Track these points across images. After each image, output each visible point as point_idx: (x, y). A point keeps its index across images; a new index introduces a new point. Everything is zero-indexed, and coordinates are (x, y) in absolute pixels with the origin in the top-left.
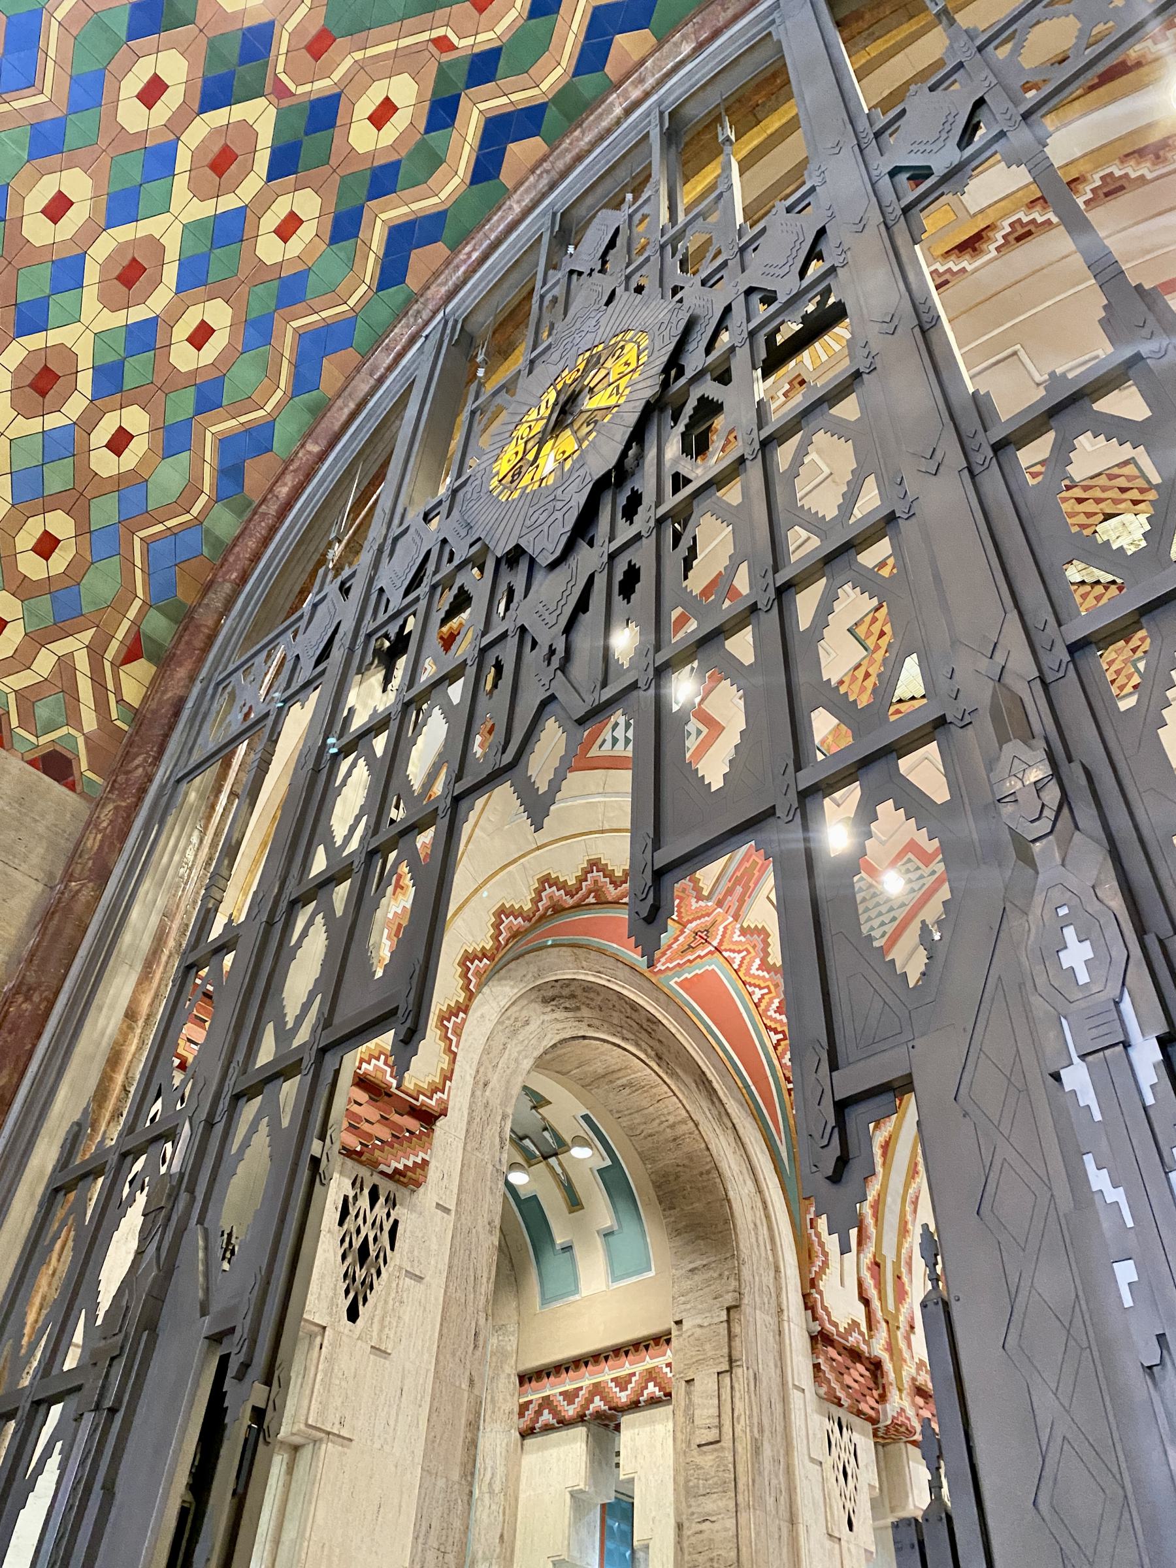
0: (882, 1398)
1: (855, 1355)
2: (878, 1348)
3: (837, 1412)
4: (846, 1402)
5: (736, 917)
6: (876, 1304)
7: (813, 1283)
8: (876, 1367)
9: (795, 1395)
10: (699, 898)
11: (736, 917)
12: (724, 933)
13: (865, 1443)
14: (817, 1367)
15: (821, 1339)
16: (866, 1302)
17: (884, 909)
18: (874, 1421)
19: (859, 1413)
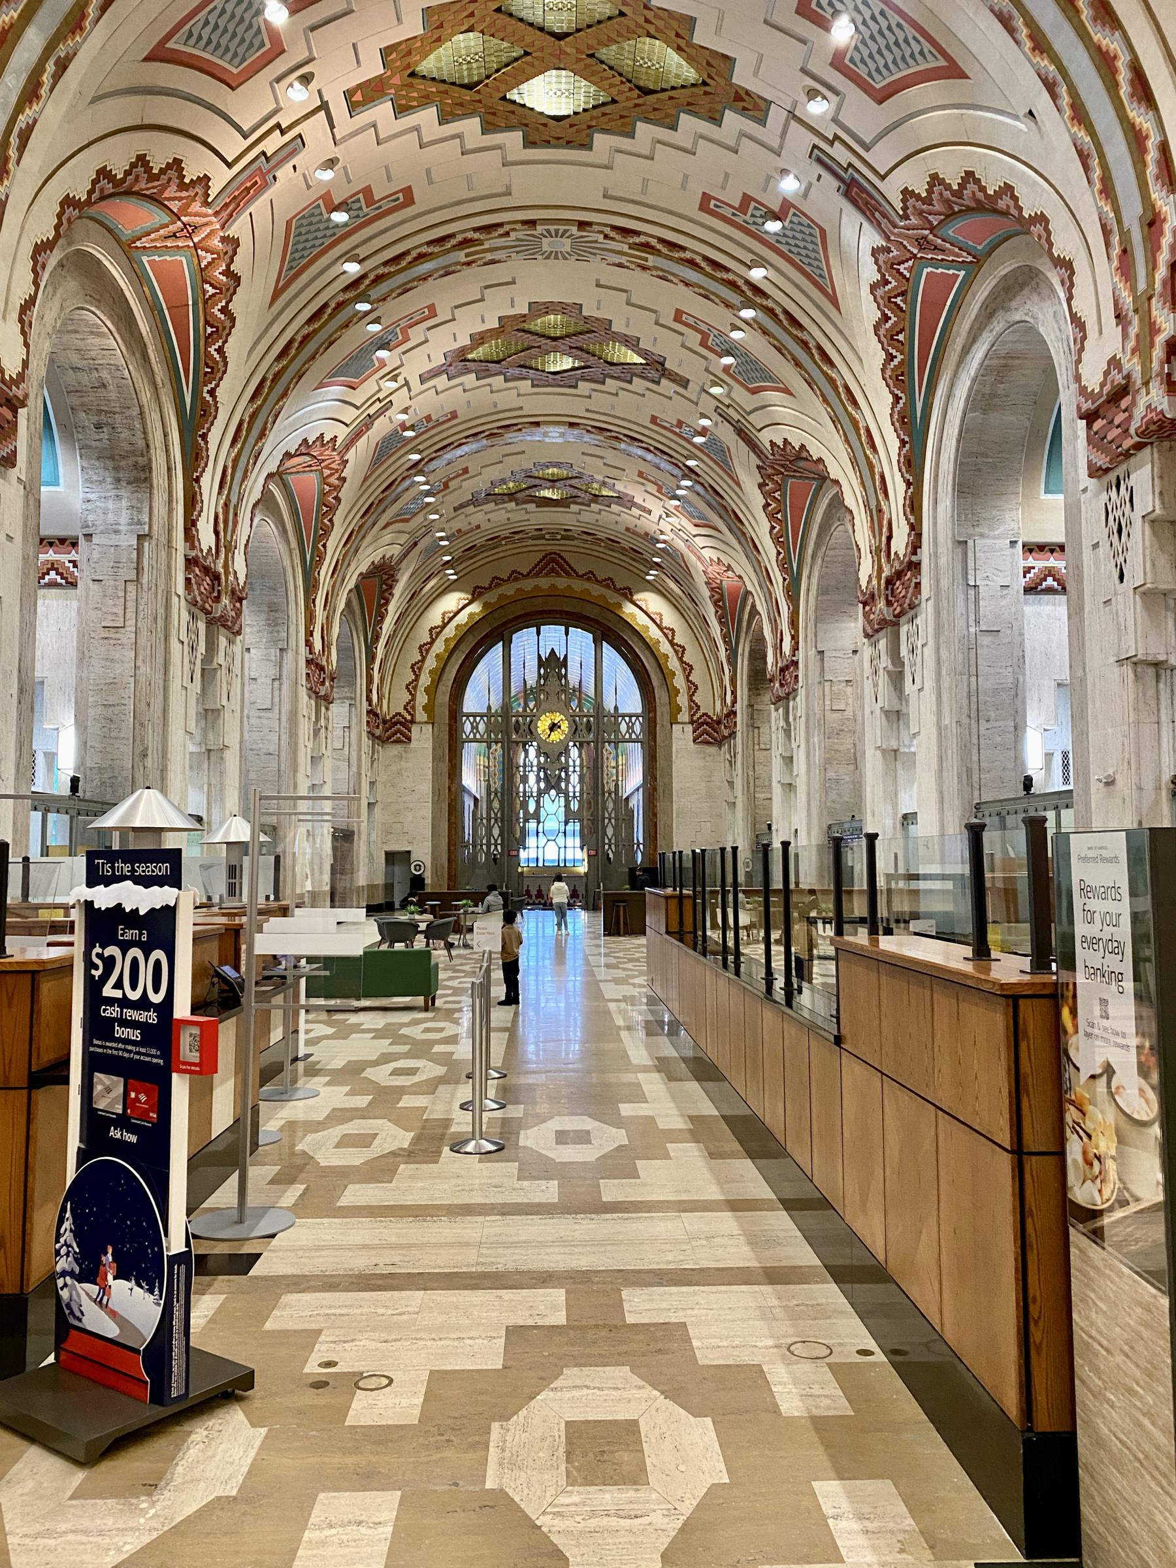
0: (217, 599)
1: (206, 570)
3: (193, 609)
4: (200, 603)
6: (222, 534)
7: (194, 523)
8: (216, 577)
9: (175, 599)
10: (206, 204)
12: (209, 234)
13: (202, 626)
14: (188, 580)
15: (190, 562)
16: (217, 533)
17: (322, 226)
18: (208, 613)
19: (203, 609)
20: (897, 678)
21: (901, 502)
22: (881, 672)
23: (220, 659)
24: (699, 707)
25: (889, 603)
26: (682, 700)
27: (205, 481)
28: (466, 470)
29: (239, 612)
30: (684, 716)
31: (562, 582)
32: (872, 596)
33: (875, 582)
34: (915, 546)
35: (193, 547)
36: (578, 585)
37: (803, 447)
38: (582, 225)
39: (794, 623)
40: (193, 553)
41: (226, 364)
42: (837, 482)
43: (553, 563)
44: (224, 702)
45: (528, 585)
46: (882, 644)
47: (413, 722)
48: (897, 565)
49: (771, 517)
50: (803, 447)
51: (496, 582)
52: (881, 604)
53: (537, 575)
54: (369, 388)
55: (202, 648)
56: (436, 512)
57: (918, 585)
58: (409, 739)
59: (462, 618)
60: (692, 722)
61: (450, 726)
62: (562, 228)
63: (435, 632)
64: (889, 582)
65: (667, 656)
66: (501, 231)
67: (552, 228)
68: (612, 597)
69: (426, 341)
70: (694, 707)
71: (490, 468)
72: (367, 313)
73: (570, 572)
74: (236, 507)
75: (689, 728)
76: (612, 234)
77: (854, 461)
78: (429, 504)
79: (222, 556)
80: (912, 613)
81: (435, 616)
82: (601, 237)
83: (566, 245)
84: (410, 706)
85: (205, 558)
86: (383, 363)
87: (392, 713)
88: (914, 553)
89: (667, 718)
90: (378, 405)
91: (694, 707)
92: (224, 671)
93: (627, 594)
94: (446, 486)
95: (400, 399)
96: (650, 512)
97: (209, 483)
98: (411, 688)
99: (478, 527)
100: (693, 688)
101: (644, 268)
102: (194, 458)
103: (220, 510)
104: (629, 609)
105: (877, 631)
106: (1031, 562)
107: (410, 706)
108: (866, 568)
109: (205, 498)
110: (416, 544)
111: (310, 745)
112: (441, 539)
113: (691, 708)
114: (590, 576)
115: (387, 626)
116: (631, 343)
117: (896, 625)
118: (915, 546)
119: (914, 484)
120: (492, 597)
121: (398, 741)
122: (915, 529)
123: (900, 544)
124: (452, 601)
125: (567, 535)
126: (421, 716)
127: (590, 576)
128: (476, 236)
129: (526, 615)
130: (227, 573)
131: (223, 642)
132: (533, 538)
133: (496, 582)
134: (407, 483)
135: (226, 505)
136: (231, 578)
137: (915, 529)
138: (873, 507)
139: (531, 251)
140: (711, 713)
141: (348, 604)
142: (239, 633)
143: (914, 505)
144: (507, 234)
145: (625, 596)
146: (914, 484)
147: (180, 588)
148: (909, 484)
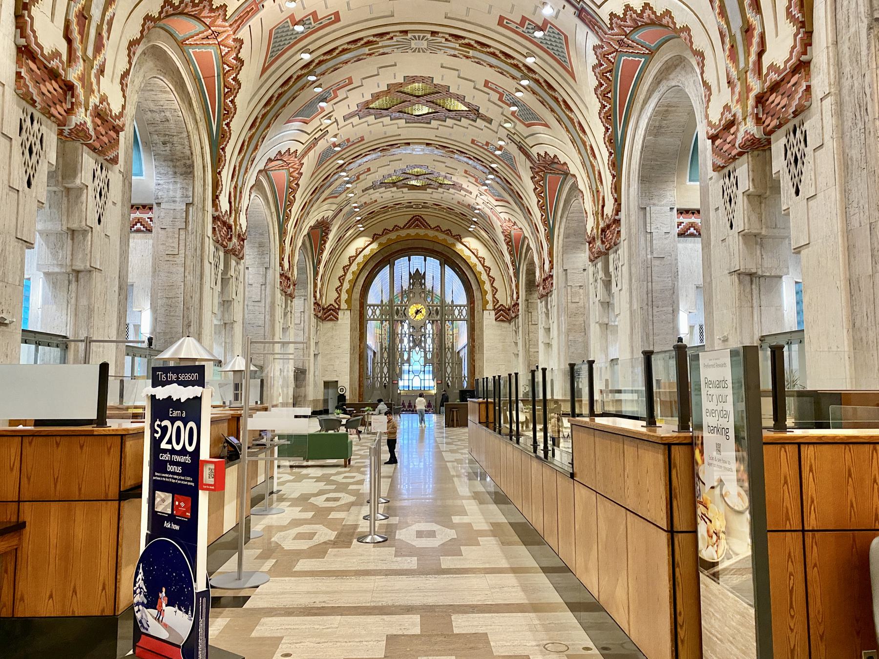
0: (230, 239)
2: (232, 222)
3: (217, 245)
5: (234, 33)
6: (233, 204)
7: (217, 197)
8: (230, 227)
9: (207, 239)
11: (234, 33)
13: (222, 254)
14: (214, 229)
15: (215, 219)
16: (230, 203)
17: (289, 33)
18: (225, 247)
19: (222, 245)
20: (607, 284)
21: (610, 186)
22: (599, 281)
23: (232, 272)
24: (498, 302)
25: (603, 242)
26: (489, 297)
27: (224, 174)
28: (369, 170)
29: (242, 247)
30: (490, 306)
31: (422, 232)
32: (594, 239)
33: (595, 231)
34: (618, 211)
35: (217, 210)
36: (431, 233)
37: (555, 156)
38: (433, 33)
39: (551, 254)
40: (216, 214)
41: (235, 109)
42: (574, 176)
43: (417, 221)
44: (234, 296)
45: (403, 233)
46: (599, 265)
47: (339, 309)
48: (607, 221)
49: (538, 195)
50: (555, 156)
51: (386, 232)
52: (599, 243)
53: (409, 228)
54: (315, 123)
55: (222, 267)
56: (352, 193)
57: (619, 232)
58: (337, 319)
59: (367, 251)
60: (494, 309)
61: (360, 311)
62: (422, 35)
63: (352, 259)
64: (603, 230)
65: (480, 273)
66: (388, 36)
67: (417, 35)
68: (450, 240)
69: (347, 97)
70: (496, 301)
71: (382, 168)
72: (314, 82)
73: (426, 226)
74: (241, 188)
75: (493, 313)
76: (450, 38)
77: (584, 164)
78: (348, 188)
79: (233, 215)
80: (615, 248)
81: (351, 251)
82: (444, 40)
83: (424, 44)
84: (338, 300)
85: (223, 217)
86: (323, 110)
87: (328, 304)
88: (617, 214)
89: (480, 307)
90: (320, 133)
91: (496, 301)
92: (234, 279)
93: (459, 238)
94: (358, 178)
95: (333, 130)
96: (471, 193)
97: (226, 175)
98: (338, 290)
99: (376, 201)
100: (495, 291)
101: (467, 57)
102: (218, 161)
103: (232, 190)
104: (459, 247)
105: (596, 258)
106: (681, 219)
107: (338, 300)
108: (590, 223)
109: (224, 183)
110: (341, 210)
111: (282, 321)
112: (355, 207)
113: (494, 302)
114: (438, 228)
115: (325, 255)
116: (461, 99)
117: (606, 254)
118: (618, 211)
119: (617, 177)
120: (384, 240)
121: (331, 320)
122: (617, 201)
123: (609, 209)
124: (361, 242)
125: (425, 206)
126: (344, 306)
127: (438, 228)
128: (375, 39)
129: (401, 250)
130: (236, 225)
131: (233, 263)
132: (407, 207)
133: (386, 232)
134: (336, 176)
135: (235, 187)
136: (238, 228)
137: (617, 201)
138: (594, 189)
139: (405, 48)
140: (505, 304)
141: (304, 243)
142: (242, 258)
143: (617, 188)
144: (392, 38)
145: (457, 239)
146: (617, 177)
147: (210, 232)
148: (614, 176)
